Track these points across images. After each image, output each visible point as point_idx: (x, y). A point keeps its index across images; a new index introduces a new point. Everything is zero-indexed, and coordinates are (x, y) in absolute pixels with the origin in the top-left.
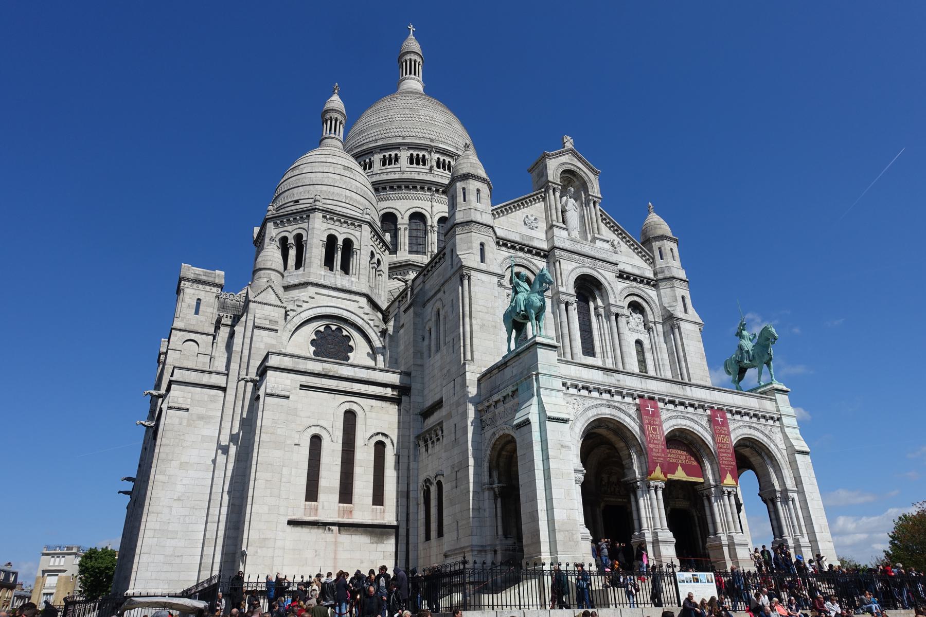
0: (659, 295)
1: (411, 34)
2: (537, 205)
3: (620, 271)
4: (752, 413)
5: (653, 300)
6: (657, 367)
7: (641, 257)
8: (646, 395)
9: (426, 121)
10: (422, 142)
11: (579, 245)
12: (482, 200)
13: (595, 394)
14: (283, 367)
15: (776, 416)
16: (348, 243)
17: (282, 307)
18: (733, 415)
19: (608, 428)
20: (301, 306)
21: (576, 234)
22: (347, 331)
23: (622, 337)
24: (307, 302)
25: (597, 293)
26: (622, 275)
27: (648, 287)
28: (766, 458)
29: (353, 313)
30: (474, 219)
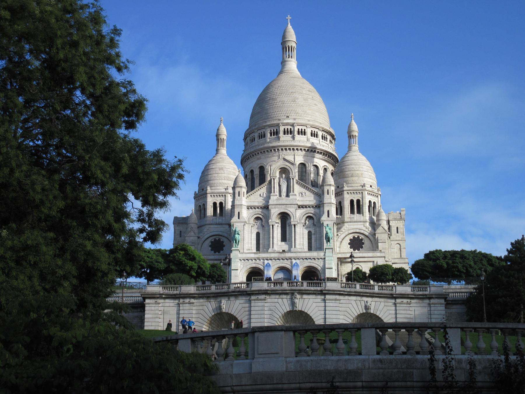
0: (320, 211)
1: (289, 23)
6: (316, 241)
8: (268, 259)
10: (275, 122)
11: (280, 201)
13: (250, 261)
16: (221, 204)
19: (256, 269)
21: (284, 193)
22: (222, 239)
23: (297, 233)
24: (206, 232)
25: (289, 217)
27: (316, 208)
29: (223, 232)
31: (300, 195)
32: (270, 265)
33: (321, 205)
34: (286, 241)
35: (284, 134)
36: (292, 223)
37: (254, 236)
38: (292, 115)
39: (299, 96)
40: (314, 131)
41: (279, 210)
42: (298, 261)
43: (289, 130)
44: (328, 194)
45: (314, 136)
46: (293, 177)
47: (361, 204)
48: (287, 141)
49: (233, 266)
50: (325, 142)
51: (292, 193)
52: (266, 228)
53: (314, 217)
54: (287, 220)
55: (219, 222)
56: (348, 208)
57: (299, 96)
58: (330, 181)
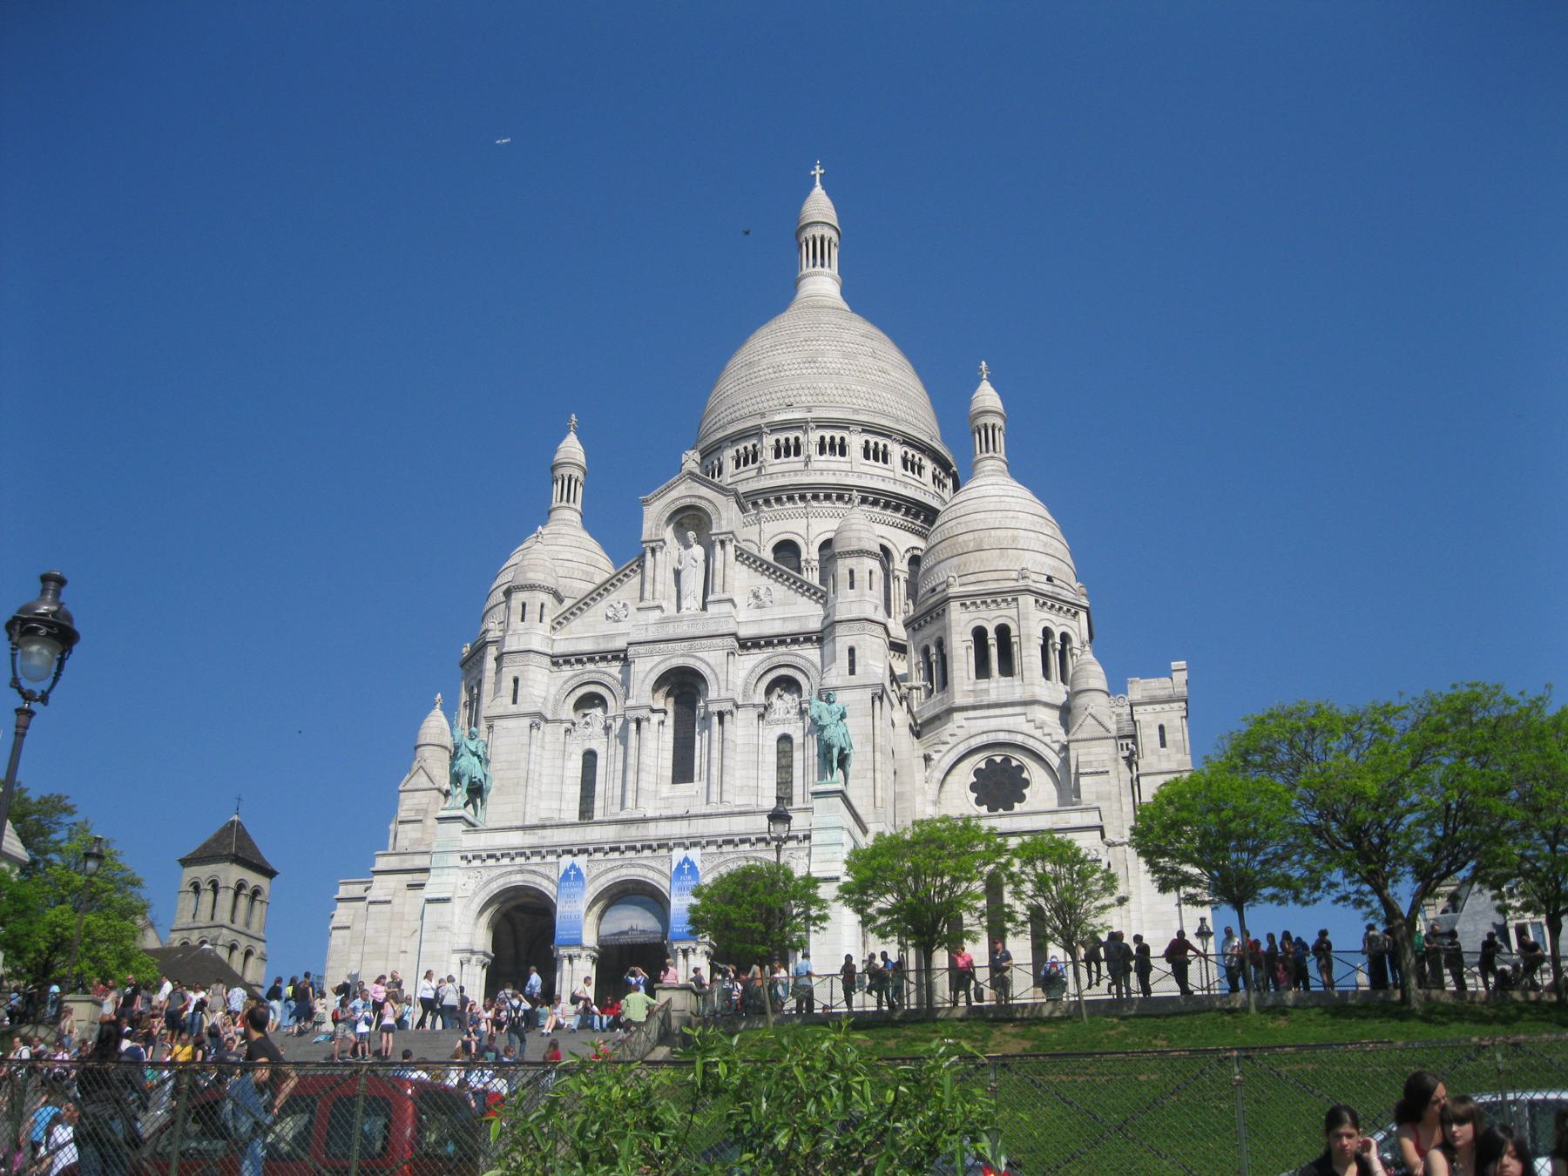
0: (822, 656)
1: (818, 183)
4: (753, 838)
5: (813, 665)
7: (810, 598)
8: (575, 849)
9: (767, 377)
10: (749, 424)
11: (671, 625)
15: (801, 835)
17: (435, 789)
18: (720, 846)
19: (528, 896)
21: (692, 603)
25: (702, 687)
27: (808, 646)
31: (753, 601)
32: (579, 875)
34: (691, 780)
35: (777, 456)
37: (575, 766)
38: (803, 398)
39: (828, 347)
40: (876, 444)
41: (665, 660)
42: (695, 854)
43: (792, 441)
44: (852, 586)
45: (876, 459)
46: (721, 537)
47: (1013, 640)
48: (783, 473)
50: (917, 477)
56: (965, 659)
57: (828, 347)
58: (859, 539)
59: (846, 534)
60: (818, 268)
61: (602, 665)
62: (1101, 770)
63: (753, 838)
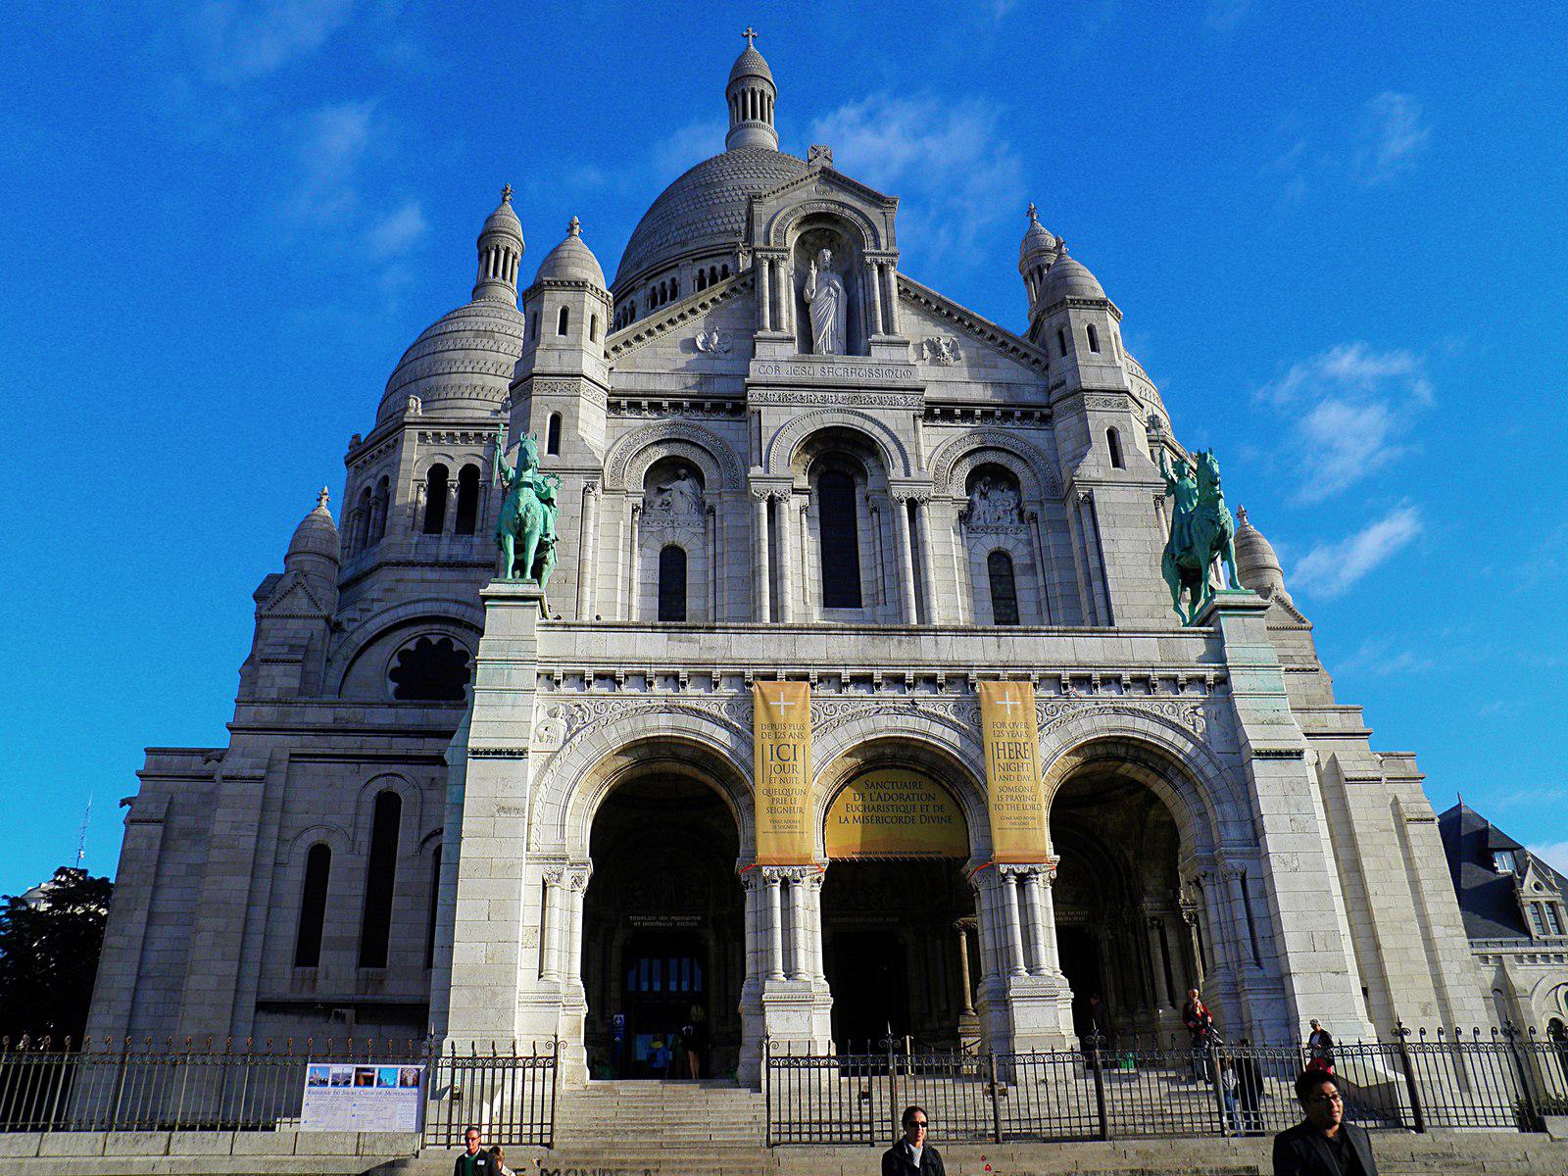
2: (734, 306)
3: (927, 403)
4: (1126, 676)
8: (782, 672)
10: (721, 241)
11: (818, 367)
12: (570, 328)
14: (255, 725)
20: (369, 611)
24: (380, 600)
25: (869, 464)
26: (940, 412)
28: (1178, 782)
29: (468, 605)
30: (535, 370)
33: (1055, 408)
34: (861, 607)
36: (899, 492)
44: (1094, 348)
49: (485, 725)
51: (881, 336)
52: (728, 522)
53: (1017, 467)
54: (859, 480)
55: (450, 556)
59: (1075, 279)
60: (758, 121)
61: (696, 417)
62: (1309, 667)
63: (1126, 676)
